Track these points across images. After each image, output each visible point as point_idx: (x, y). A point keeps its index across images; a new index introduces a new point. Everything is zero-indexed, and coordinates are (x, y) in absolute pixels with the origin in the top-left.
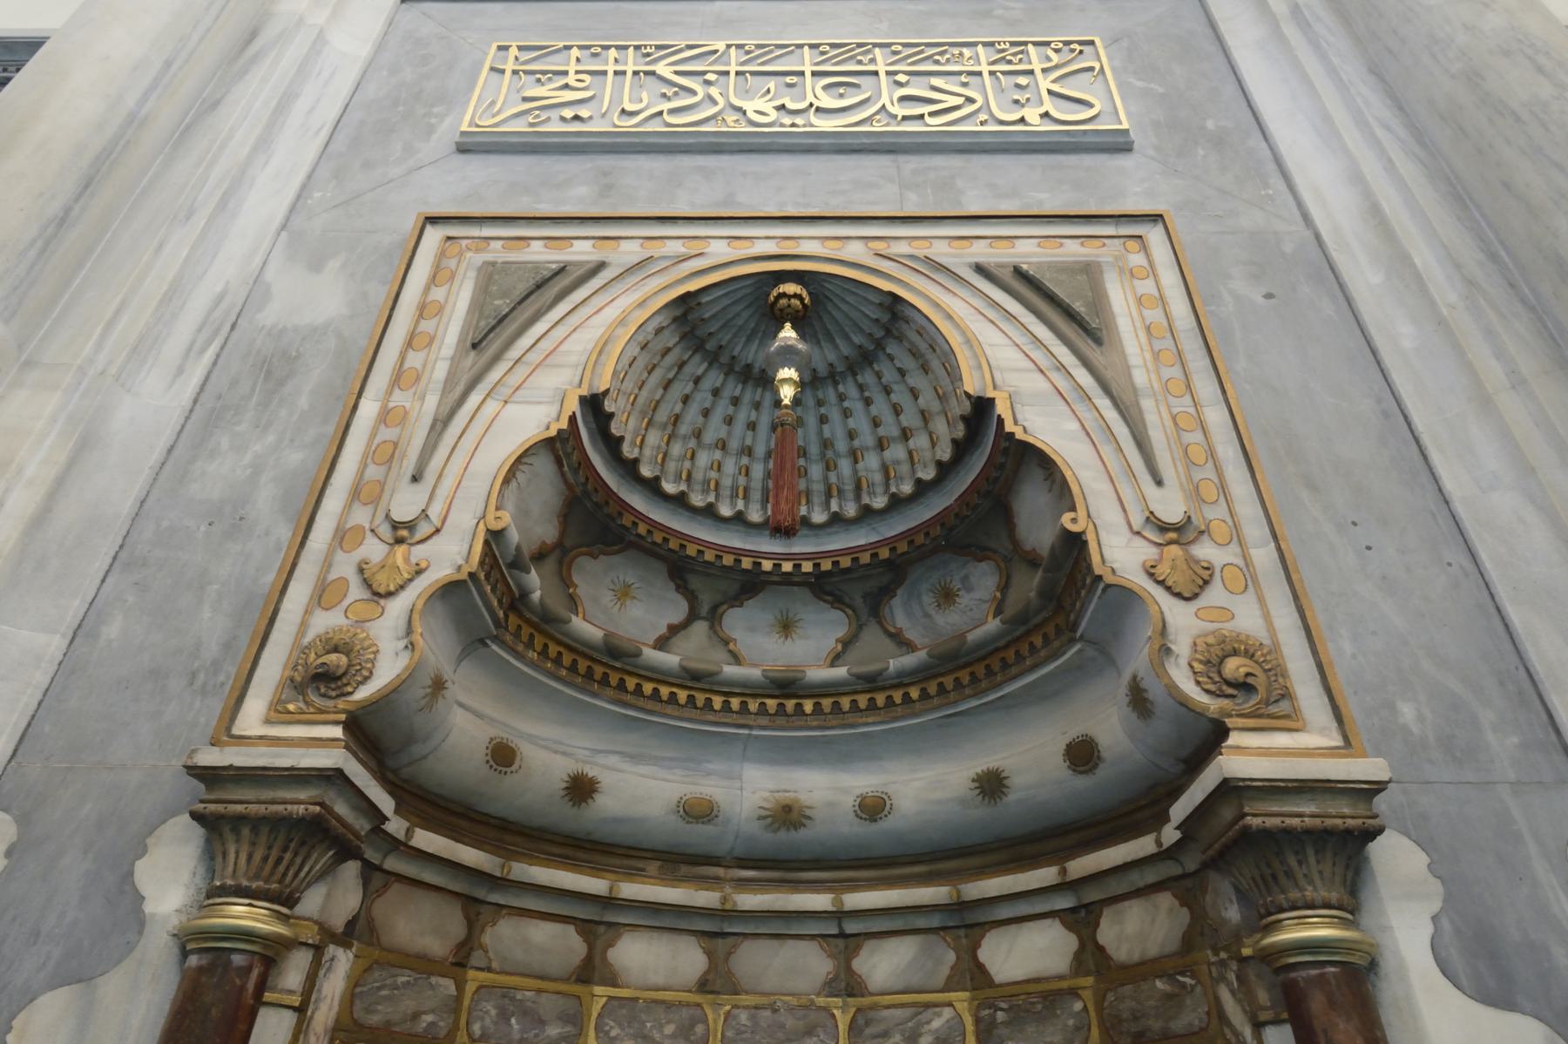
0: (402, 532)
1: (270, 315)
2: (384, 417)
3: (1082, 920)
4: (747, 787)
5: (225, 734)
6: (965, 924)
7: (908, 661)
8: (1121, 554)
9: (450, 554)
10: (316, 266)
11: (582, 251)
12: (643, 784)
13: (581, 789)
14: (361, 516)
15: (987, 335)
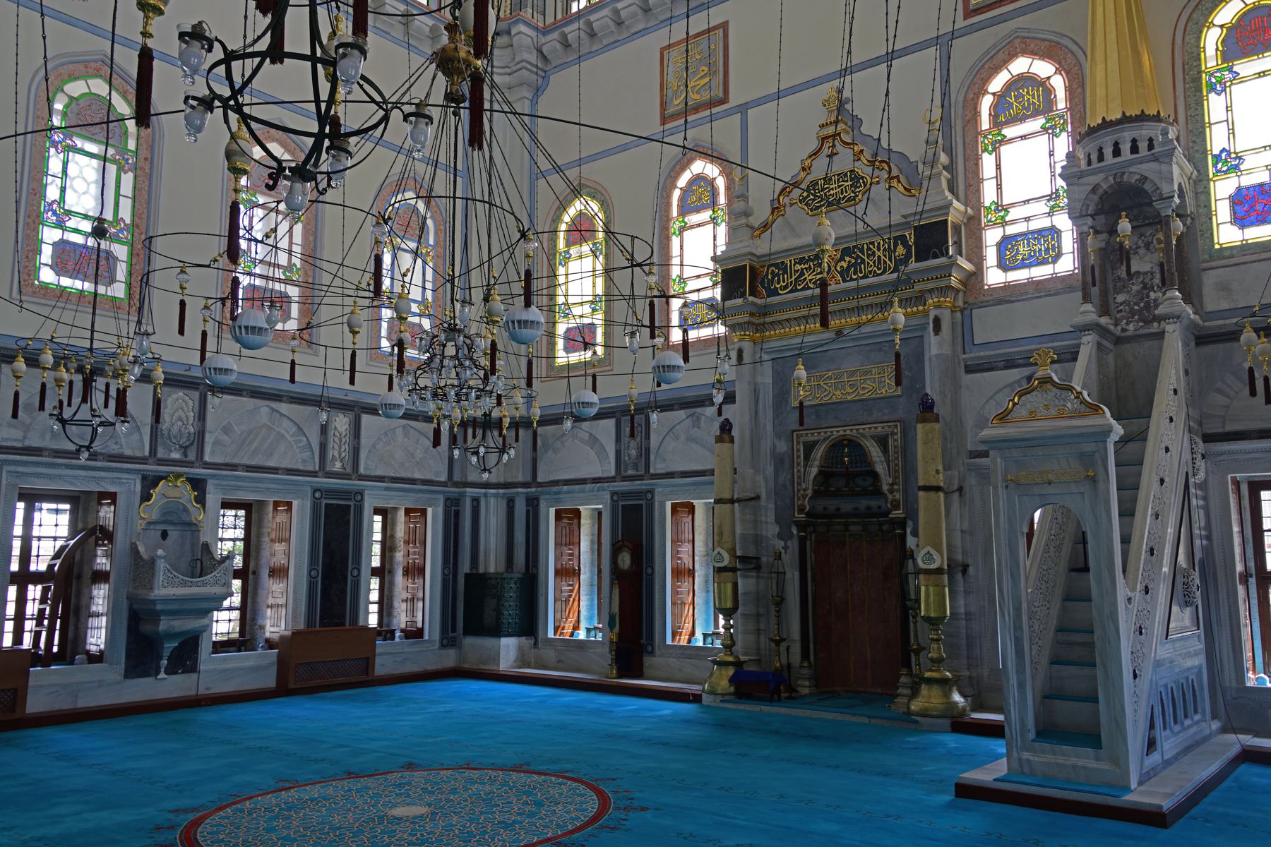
1: (778, 450)
8: (885, 488)
9: (810, 492)
12: (847, 507)
13: (838, 509)
15: (872, 449)
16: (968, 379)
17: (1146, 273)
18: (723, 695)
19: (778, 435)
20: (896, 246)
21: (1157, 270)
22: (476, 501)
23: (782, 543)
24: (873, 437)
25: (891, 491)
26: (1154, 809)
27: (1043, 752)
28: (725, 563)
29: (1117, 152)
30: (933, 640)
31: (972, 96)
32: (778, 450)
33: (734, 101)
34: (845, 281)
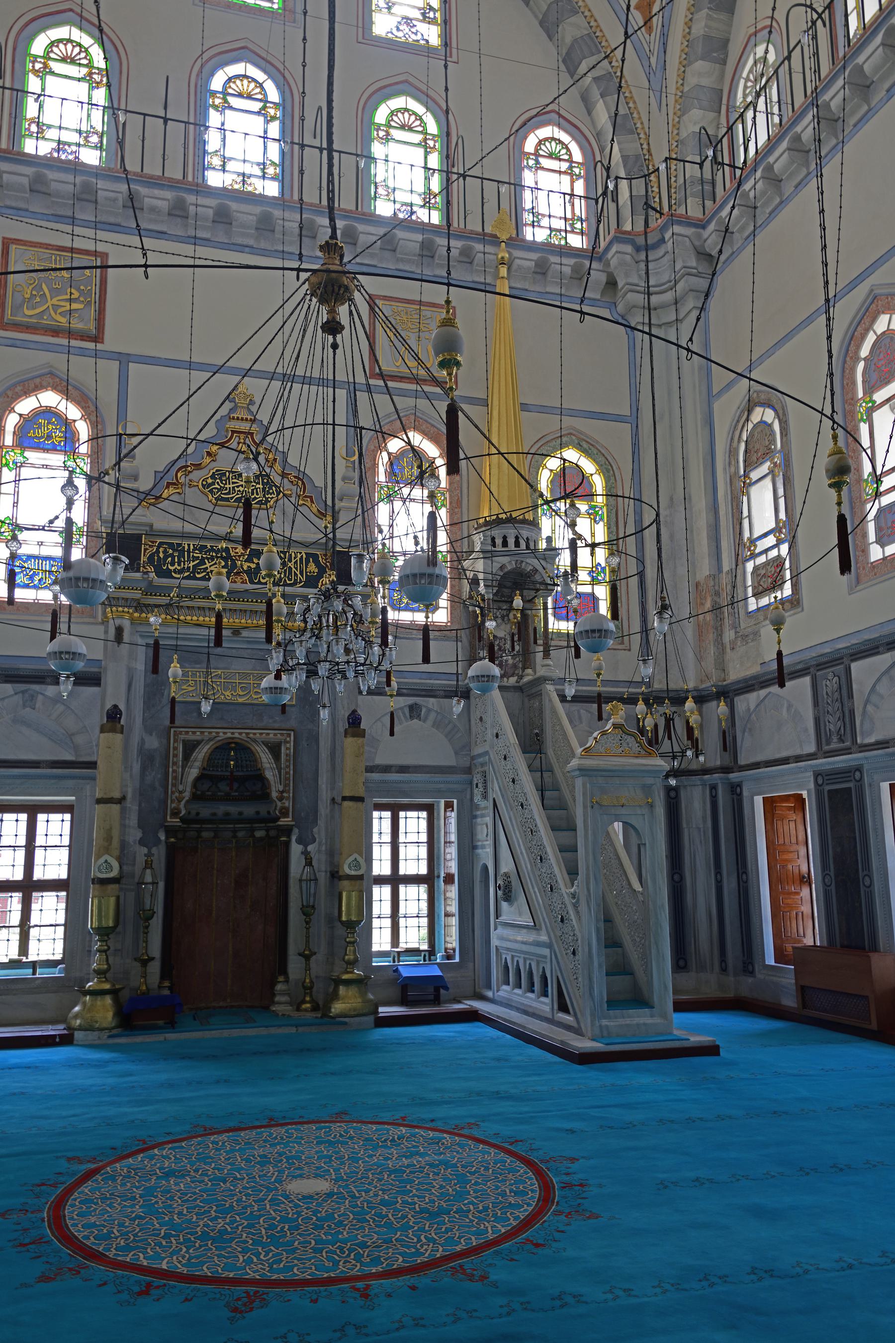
0: (181, 792)
1: (147, 746)
2: (174, 771)
3: (267, 831)
4: (222, 809)
5: (166, 821)
6: (253, 830)
7: (248, 794)
8: (274, 795)
9: (187, 795)
10: (151, 735)
11: (198, 736)
12: (205, 811)
13: (198, 814)
14: (174, 789)
15: (262, 755)
17: (501, 638)
18: (110, 1029)
19: (148, 729)
20: (307, 562)
21: (508, 638)
23: (145, 850)
24: (266, 744)
25: (281, 799)
26: (711, 1044)
27: (616, 1017)
28: (114, 873)
30: (350, 943)
31: (372, 447)
32: (147, 746)
33: (110, 343)
34: (252, 582)
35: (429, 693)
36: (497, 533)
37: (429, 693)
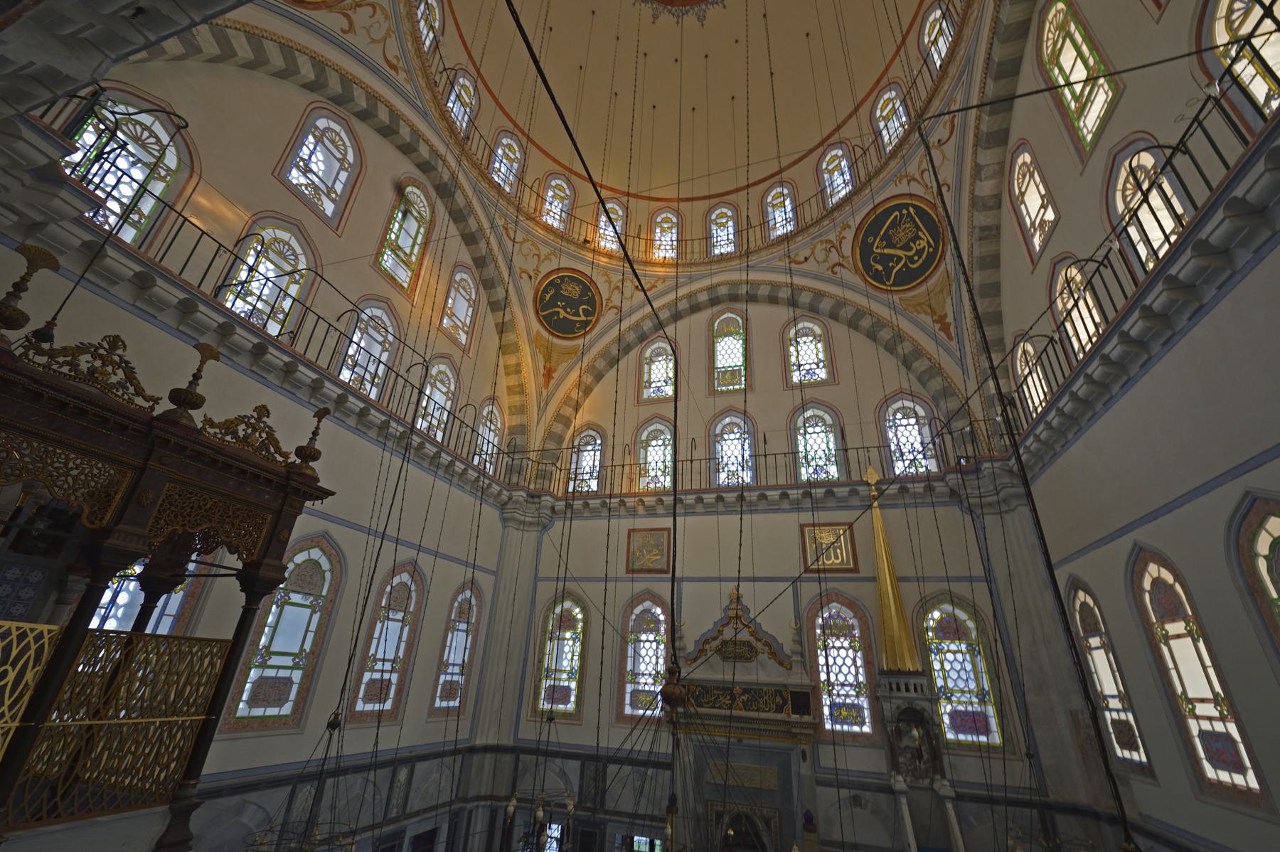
16: (819, 789)
22: (471, 812)
29: (907, 690)
35: (865, 787)
36: (894, 681)
37: (865, 787)
